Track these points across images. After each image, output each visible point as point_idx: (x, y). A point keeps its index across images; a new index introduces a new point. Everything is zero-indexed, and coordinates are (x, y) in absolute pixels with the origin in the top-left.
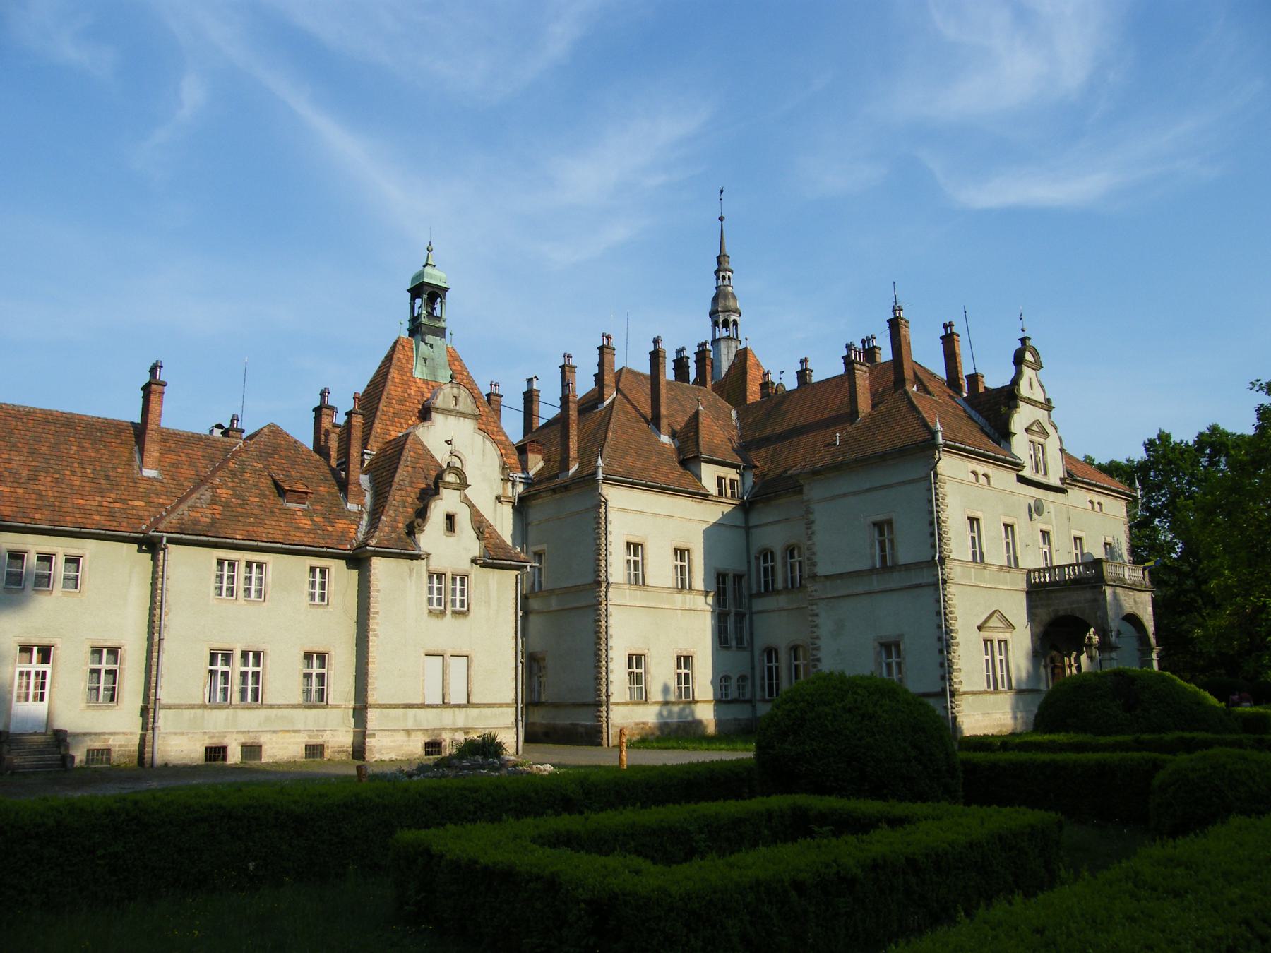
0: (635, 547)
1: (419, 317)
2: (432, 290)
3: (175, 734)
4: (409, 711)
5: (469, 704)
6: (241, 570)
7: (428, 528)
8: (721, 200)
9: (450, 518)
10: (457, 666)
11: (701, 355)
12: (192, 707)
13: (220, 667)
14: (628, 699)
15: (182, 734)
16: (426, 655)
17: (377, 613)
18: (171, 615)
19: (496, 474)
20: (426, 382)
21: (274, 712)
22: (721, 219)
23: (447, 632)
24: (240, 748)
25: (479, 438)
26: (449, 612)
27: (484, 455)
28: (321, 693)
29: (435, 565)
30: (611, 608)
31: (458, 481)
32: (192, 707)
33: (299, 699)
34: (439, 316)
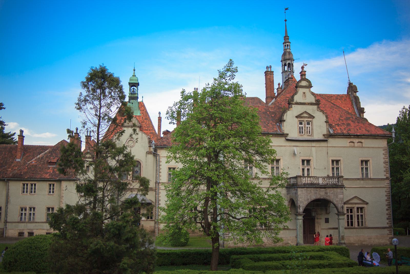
2: (132, 84)
3: (10, 229)
6: (29, 185)
8: (285, 12)
12: (15, 222)
13: (24, 212)
15: (12, 229)
17: (63, 197)
18: (10, 199)
19: (147, 145)
21: (38, 224)
22: (286, 21)
24: (27, 233)
27: (142, 139)
30: (160, 191)
31: (90, 156)
32: (15, 222)
33: (45, 221)
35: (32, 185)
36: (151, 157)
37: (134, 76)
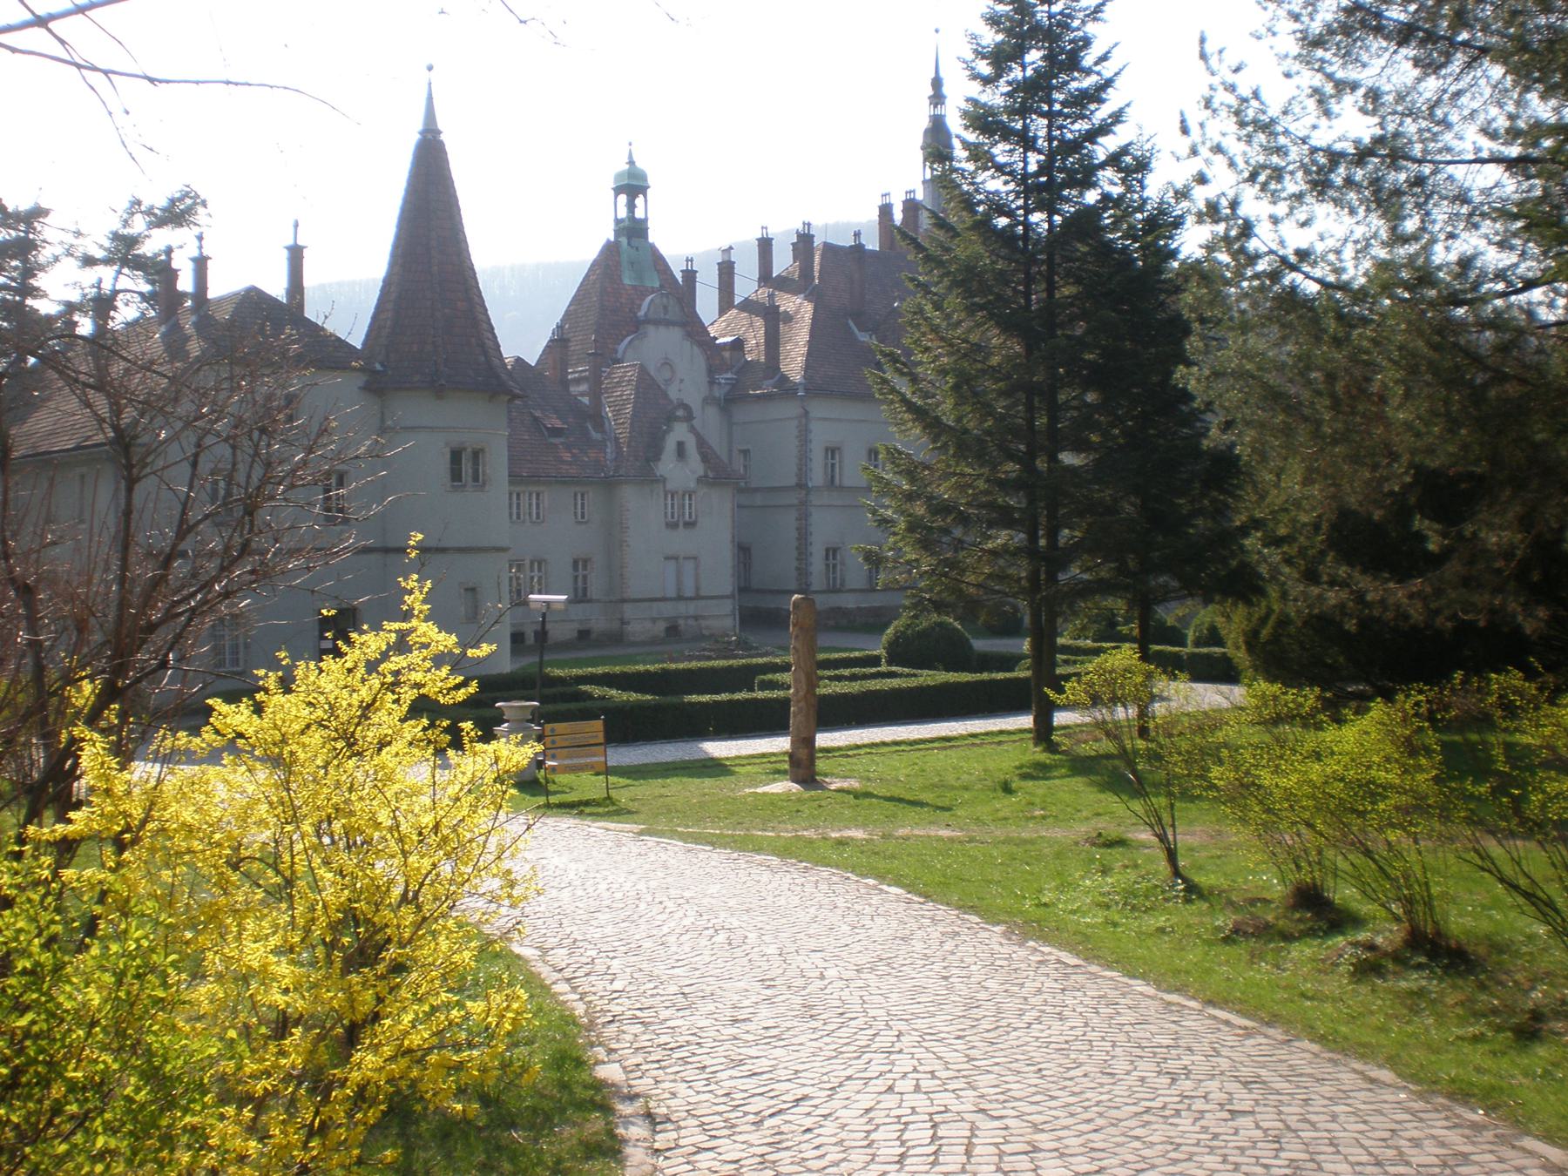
0: (832, 451)
1: (622, 220)
4: (655, 604)
5: (698, 597)
7: (664, 457)
9: (681, 448)
10: (689, 567)
11: (911, 206)
14: (825, 587)
16: (666, 558)
20: (634, 287)
22: (937, 31)
23: (680, 541)
25: (687, 344)
26: (681, 524)
28: (585, 590)
29: (669, 486)
34: (643, 216)
35: (530, 495)
36: (712, 413)
37: (631, 162)
